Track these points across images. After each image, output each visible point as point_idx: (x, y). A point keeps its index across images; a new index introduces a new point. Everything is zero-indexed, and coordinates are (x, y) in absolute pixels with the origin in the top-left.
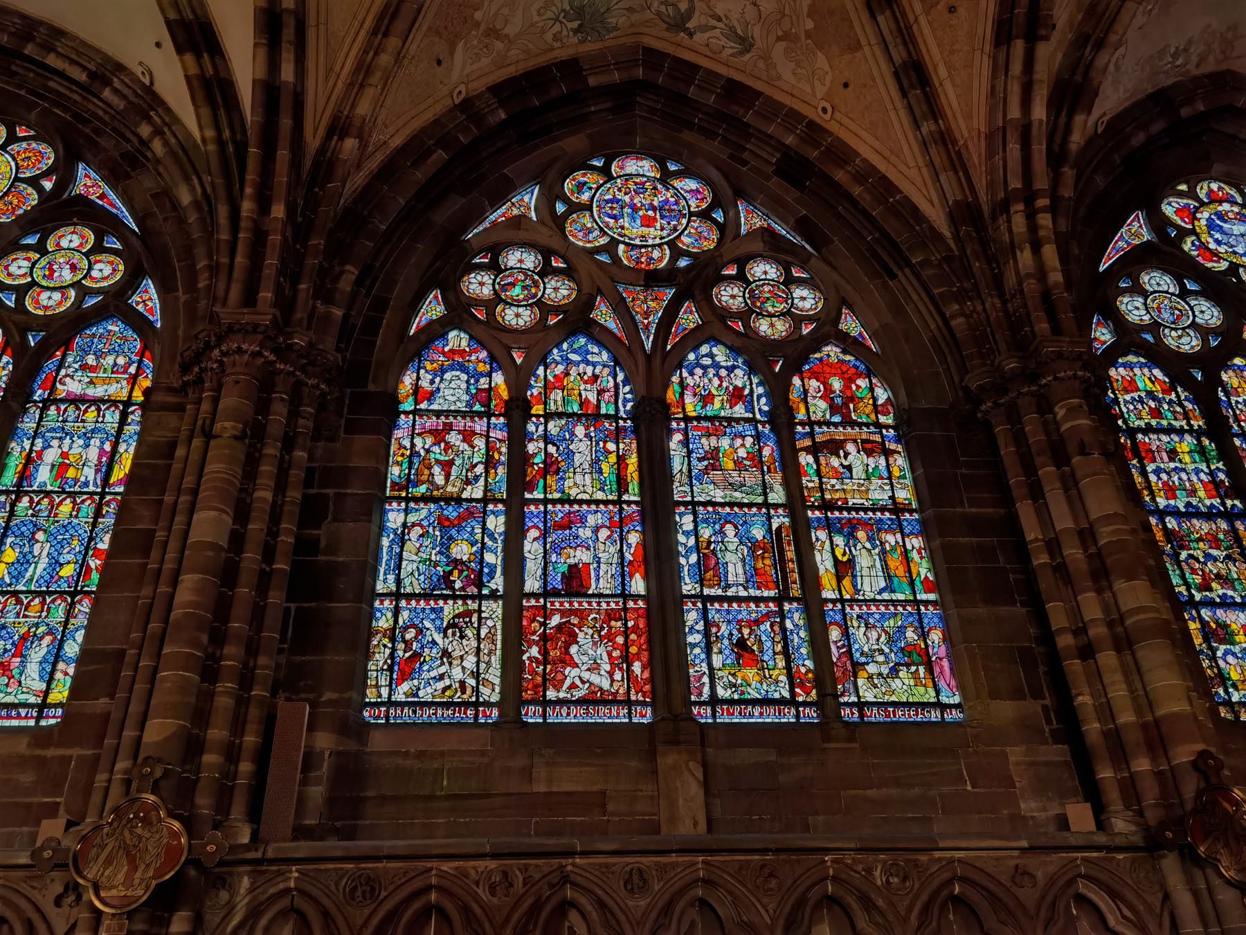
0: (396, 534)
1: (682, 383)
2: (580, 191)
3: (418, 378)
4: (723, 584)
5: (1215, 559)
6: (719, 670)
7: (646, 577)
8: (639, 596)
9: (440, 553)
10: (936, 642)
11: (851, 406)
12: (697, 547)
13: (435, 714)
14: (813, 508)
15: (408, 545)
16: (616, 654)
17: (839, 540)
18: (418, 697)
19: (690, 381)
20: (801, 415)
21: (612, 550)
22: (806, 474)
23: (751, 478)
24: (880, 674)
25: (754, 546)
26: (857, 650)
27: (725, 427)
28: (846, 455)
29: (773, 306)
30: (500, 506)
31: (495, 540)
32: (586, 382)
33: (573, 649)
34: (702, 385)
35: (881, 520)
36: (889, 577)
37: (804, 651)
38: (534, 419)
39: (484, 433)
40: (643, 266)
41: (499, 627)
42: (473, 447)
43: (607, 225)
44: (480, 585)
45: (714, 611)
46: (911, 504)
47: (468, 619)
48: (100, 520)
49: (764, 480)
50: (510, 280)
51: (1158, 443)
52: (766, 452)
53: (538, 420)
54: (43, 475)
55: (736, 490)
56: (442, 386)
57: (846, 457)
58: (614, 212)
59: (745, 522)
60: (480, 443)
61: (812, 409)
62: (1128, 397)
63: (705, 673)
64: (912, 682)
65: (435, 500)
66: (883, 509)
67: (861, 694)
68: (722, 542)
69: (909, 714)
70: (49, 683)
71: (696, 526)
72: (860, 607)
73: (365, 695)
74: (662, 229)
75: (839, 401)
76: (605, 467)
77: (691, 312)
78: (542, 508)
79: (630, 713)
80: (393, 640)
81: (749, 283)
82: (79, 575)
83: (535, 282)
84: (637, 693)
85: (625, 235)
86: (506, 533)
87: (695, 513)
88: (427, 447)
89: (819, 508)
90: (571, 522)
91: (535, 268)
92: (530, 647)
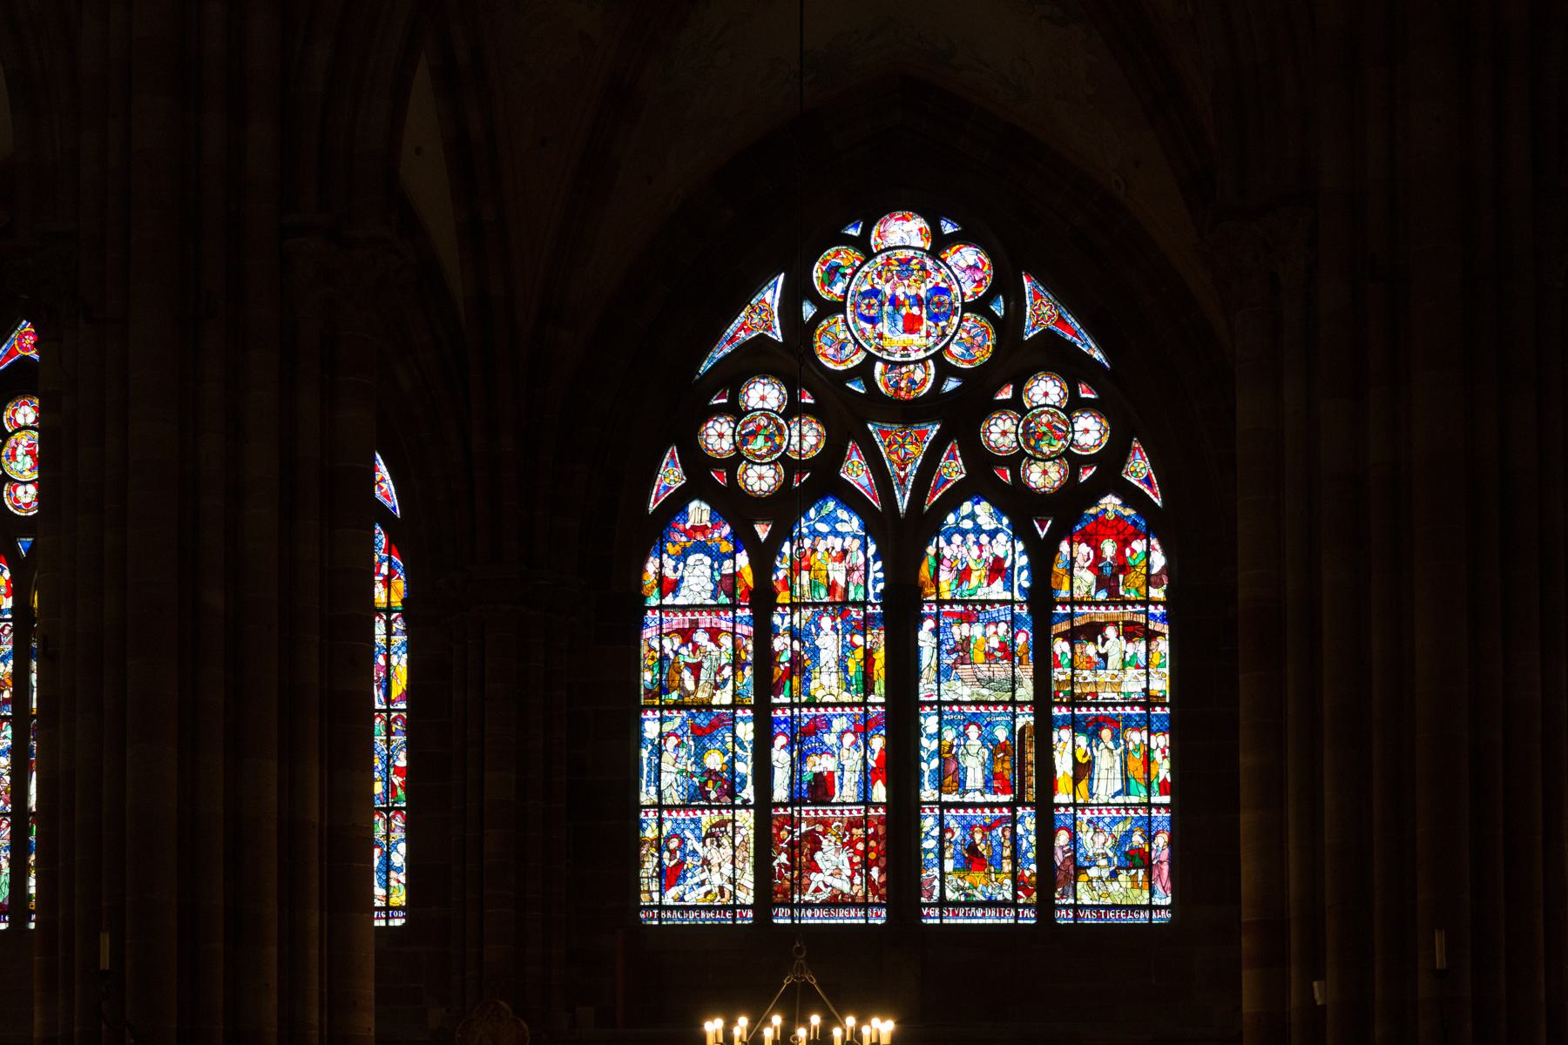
0: (653, 745)
1: (939, 558)
2: (831, 283)
3: (662, 565)
4: (960, 789)
6: (950, 874)
7: (886, 785)
8: (880, 804)
9: (694, 763)
10: (1161, 846)
11: (1121, 577)
12: (939, 752)
13: (700, 916)
14: (1060, 704)
15: (665, 757)
16: (857, 859)
17: (1082, 740)
18: (684, 901)
19: (947, 552)
20: (1064, 593)
21: (857, 756)
22: (1059, 665)
23: (1001, 670)
24: (1100, 878)
25: (996, 748)
26: (1082, 854)
27: (979, 612)
28: (1105, 640)
29: (1050, 445)
30: (749, 712)
31: (743, 748)
32: (834, 560)
33: (818, 856)
34: (959, 557)
35: (1129, 716)
36: (1126, 780)
37: (1031, 855)
38: (780, 609)
39: (731, 630)
40: (903, 393)
41: (752, 836)
42: (720, 647)
43: (862, 331)
44: (733, 794)
45: (950, 817)
46: (1164, 697)
47: (723, 829)
48: (392, 738)
49: (1013, 672)
50: (751, 427)
52: (1021, 639)
53: (784, 610)
55: (984, 687)
56: (686, 574)
57: (1103, 645)
58: (872, 312)
59: (989, 724)
60: (726, 641)
61: (1076, 583)
63: (936, 877)
64: (1129, 885)
65: (687, 708)
66: (1133, 704)
67: (1078, 897)
68: (964, 745)
69: (1119, 916)
70: (388, 890)
71: (940, 729)
72: (1092, 811)
73: (640, 900)
74: (928, 335)
75: (1108, 571)
76: (851, 664)
77: (955, 458)
78: (788, 712)
79: (866, 914)
80: (660, 850)
81: (1023, 411)
82: (387, 791)
83: (779, 428)
84: (874, 895)
85: (884, 349)
86: (755, 742)
87: (940, 714)
88: (675, 649)
89: (1067, 705)
90: (817, 728)
91: (779, 407)
92: (779, 854)
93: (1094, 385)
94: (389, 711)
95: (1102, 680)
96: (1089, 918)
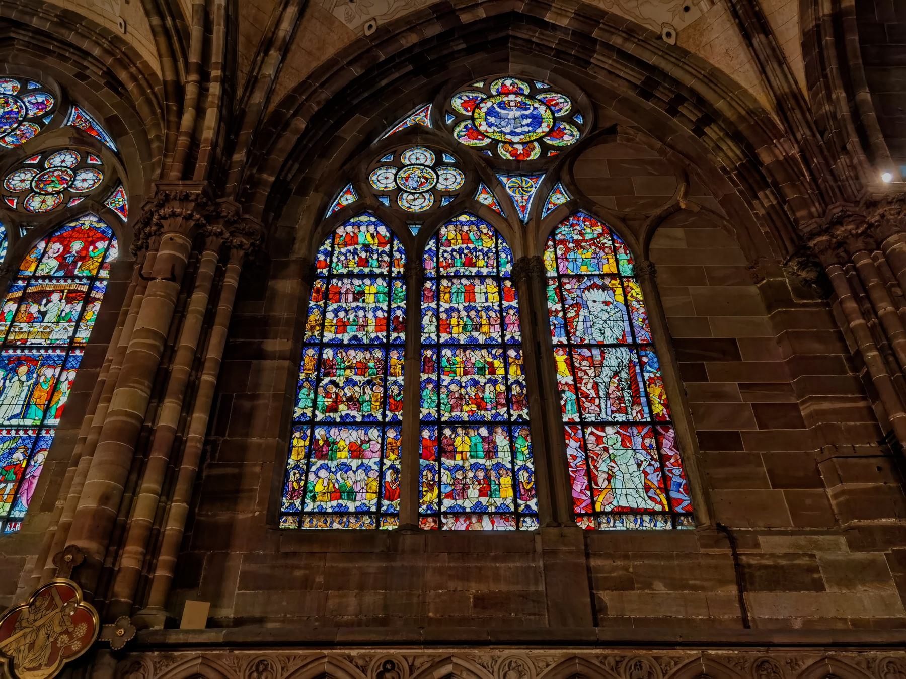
5: (355, 384)
28: (49, 302)
51: (349, 286)
57: (46, 305)
62: (344, 250)
95: (35, 330)
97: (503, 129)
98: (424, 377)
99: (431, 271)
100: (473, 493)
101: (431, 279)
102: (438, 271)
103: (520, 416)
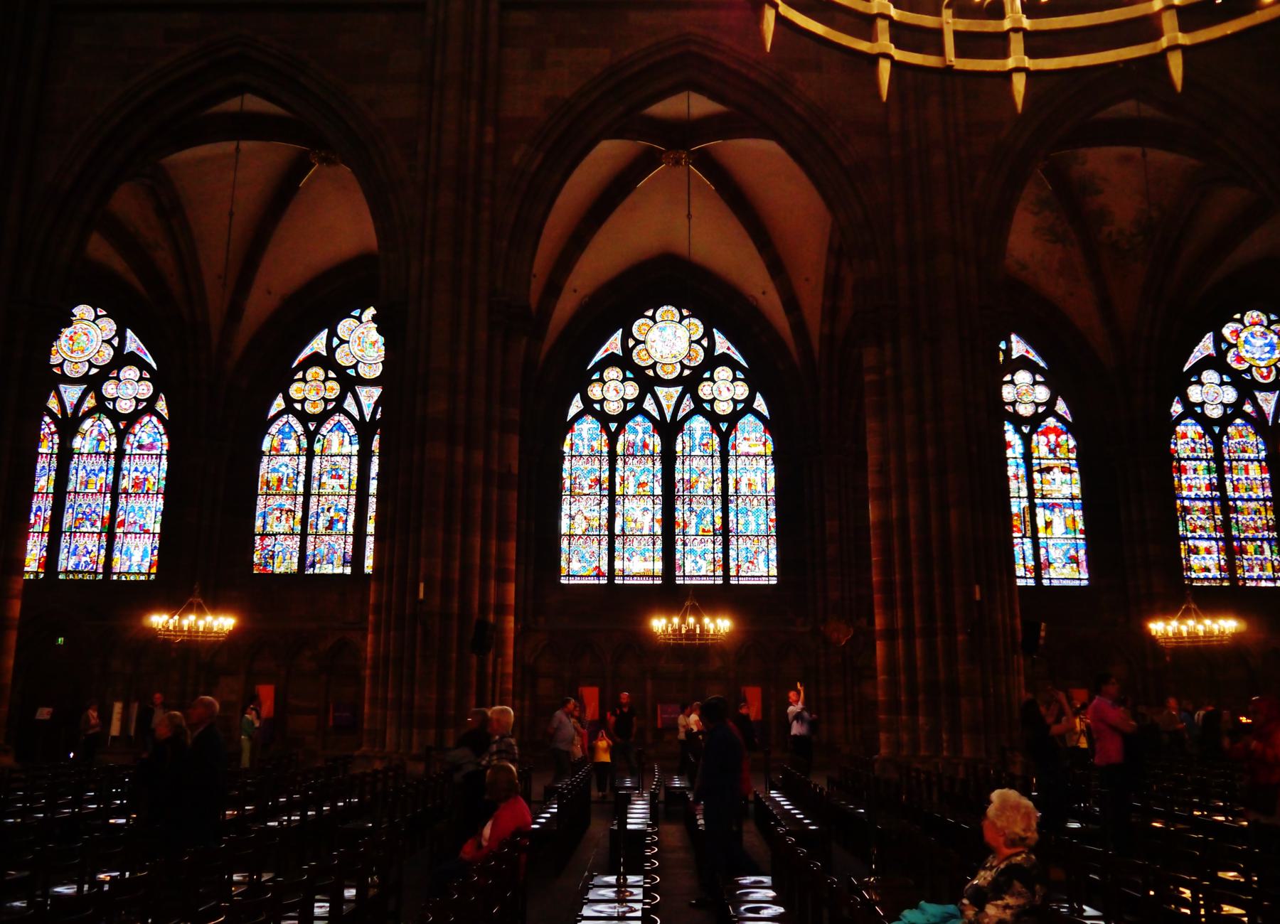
11: (1058, 449)
17: (1048, 512)
20: (1035, 455)
54: (744, 489)
66: (1067, 498)
75: (1052, 447)
93: (1042, 375)
94: (767, 496)
96: (1055, 583)
97: (1255, 356)
98: (1231, 515)
99: (1226, 456)
100: (1257, 569)
101: (1227, 460)
102: (1230, 456)
103: (1273, 536)
